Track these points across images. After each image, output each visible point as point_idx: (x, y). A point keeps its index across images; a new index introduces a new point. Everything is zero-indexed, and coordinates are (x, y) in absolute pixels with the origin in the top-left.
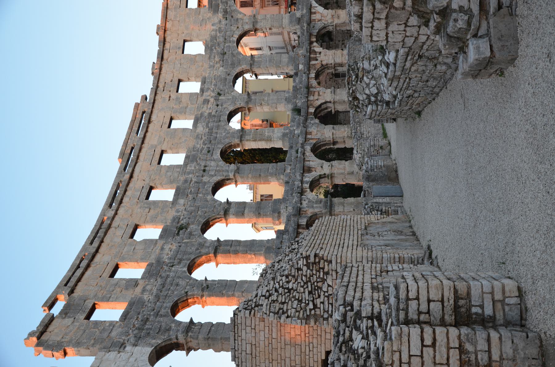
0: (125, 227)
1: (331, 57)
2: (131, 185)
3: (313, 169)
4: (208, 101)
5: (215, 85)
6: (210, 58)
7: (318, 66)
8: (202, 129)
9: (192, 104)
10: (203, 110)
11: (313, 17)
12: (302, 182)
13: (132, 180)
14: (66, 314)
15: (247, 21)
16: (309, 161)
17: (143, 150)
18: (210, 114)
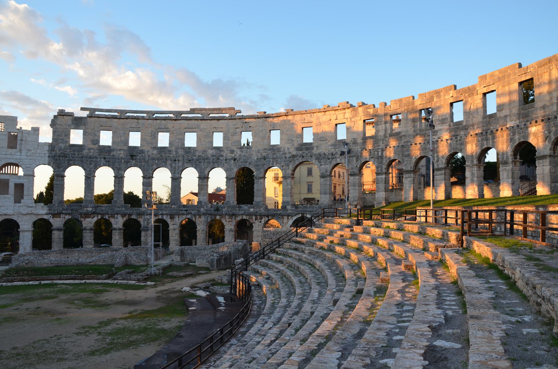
0: (138, 126)
1: (257, 229)
2: (169, 121)
3: (172, 220)
4: (232, 153)
5: (245, 156)
6: (265, 149)
7: (251, 221)
8: (211, 153)
9: (231, 144)
10: (226, 152)
11: (286, 218)
12: (162, 214)
13: (174, 121)
14: (75, 120)
15: (287, 172)
16: (179, 217)
17: (196, 122)
18: (222, 156)
